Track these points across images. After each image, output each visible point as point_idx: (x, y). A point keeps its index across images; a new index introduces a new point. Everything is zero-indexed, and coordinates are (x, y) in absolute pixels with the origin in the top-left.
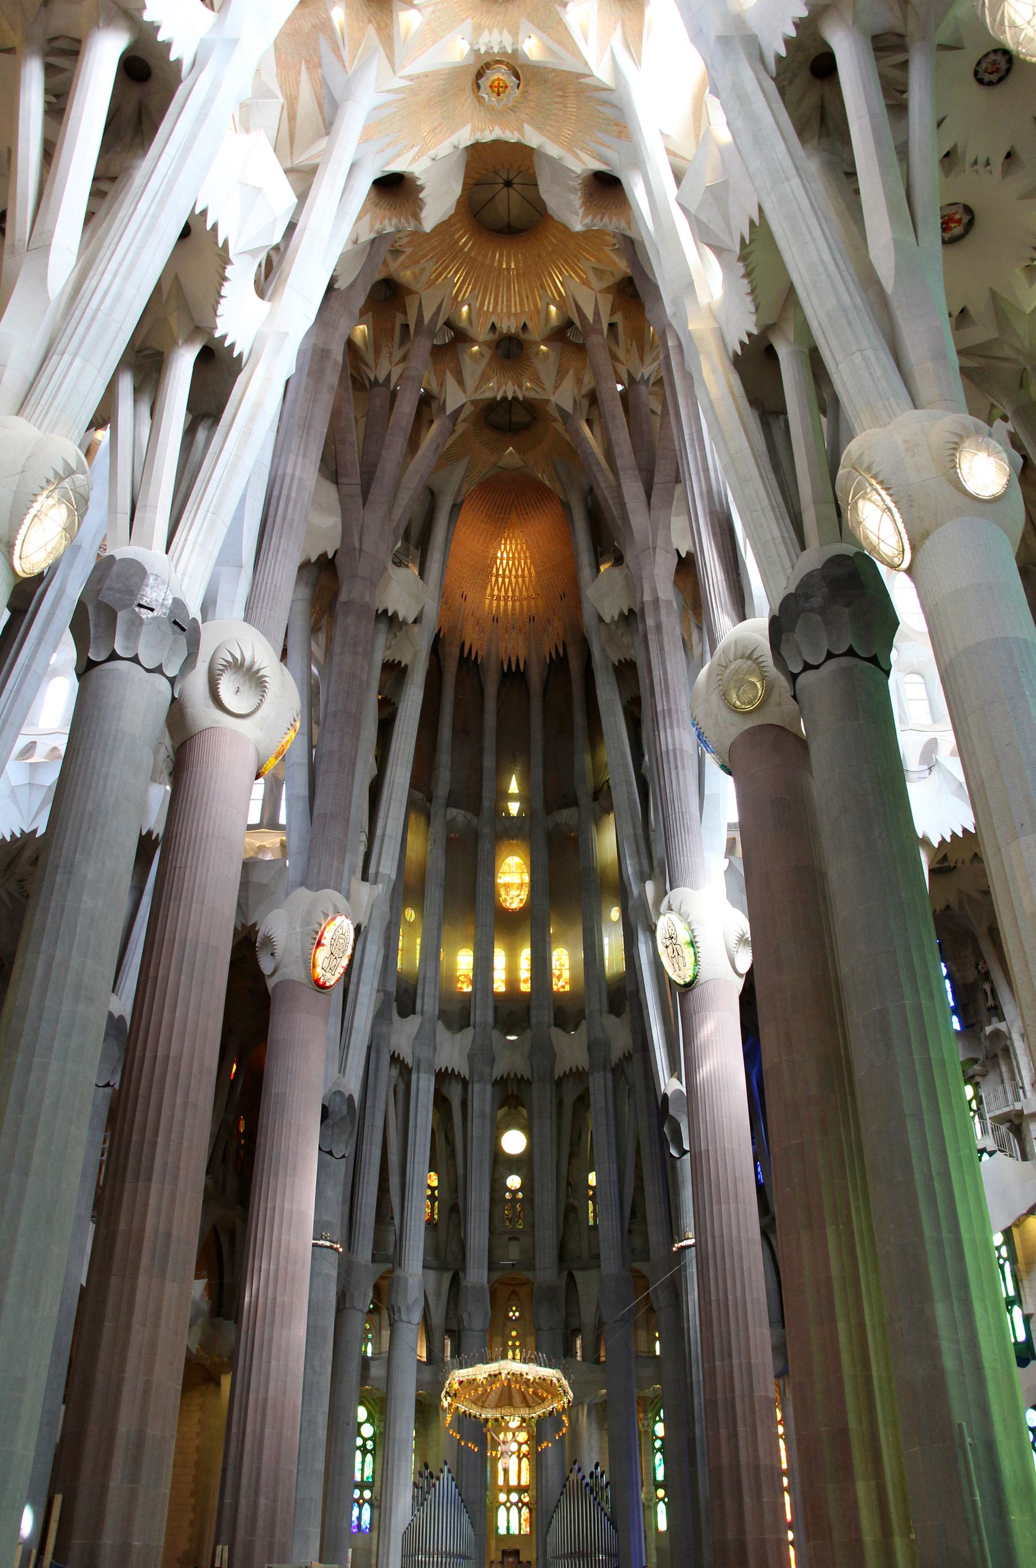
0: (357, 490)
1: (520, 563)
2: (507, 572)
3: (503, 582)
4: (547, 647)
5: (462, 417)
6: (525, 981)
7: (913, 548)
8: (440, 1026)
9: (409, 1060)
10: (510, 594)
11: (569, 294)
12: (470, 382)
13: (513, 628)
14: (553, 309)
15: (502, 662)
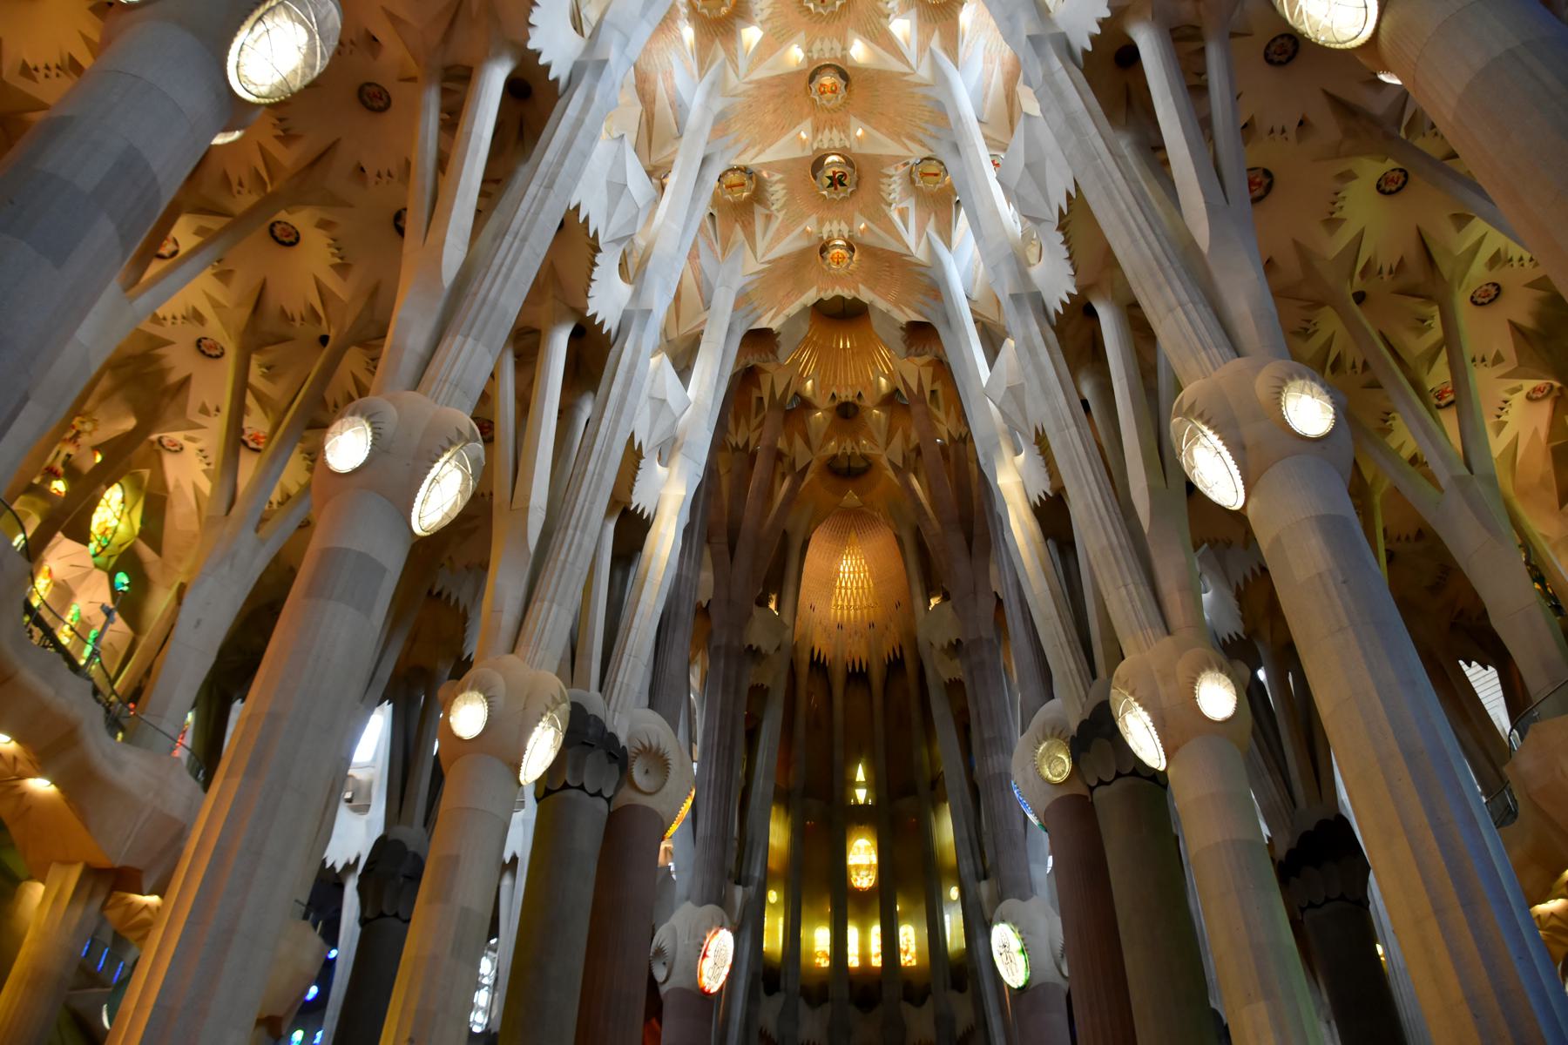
0: (725, 548)
1: (859, 576)
2: (849, 584)
3: (846, 593)
4: (887, 649)
5: (810, 470)
6: (877, 956)
7: (1167, 757)
8: (802, 1002)
9: (775, 1037)
10: (852, 603)
11: (897, 368)
12: (815, 443)
13: (856, 633)
14: (883, 381)
15: (847, 665)
